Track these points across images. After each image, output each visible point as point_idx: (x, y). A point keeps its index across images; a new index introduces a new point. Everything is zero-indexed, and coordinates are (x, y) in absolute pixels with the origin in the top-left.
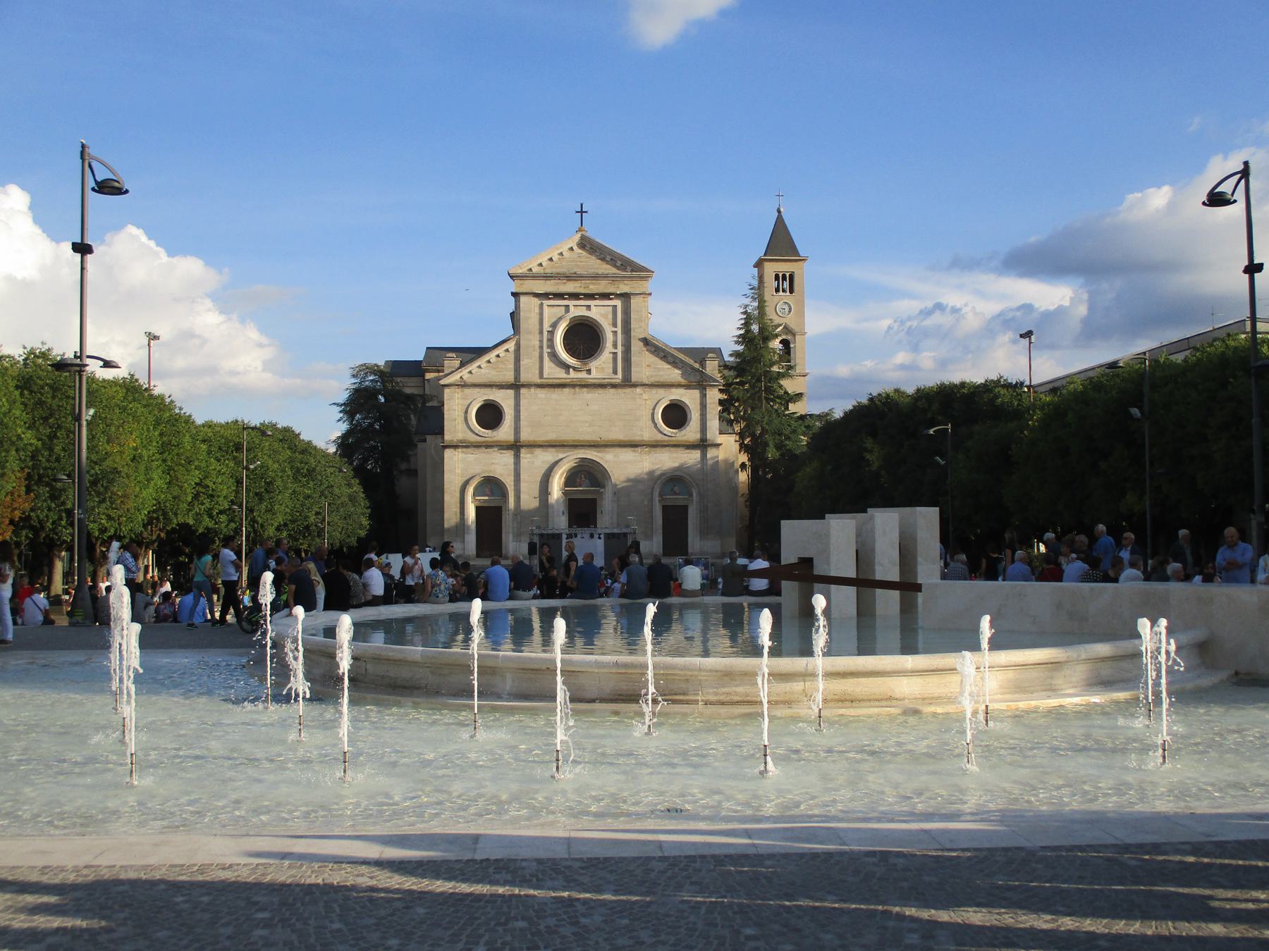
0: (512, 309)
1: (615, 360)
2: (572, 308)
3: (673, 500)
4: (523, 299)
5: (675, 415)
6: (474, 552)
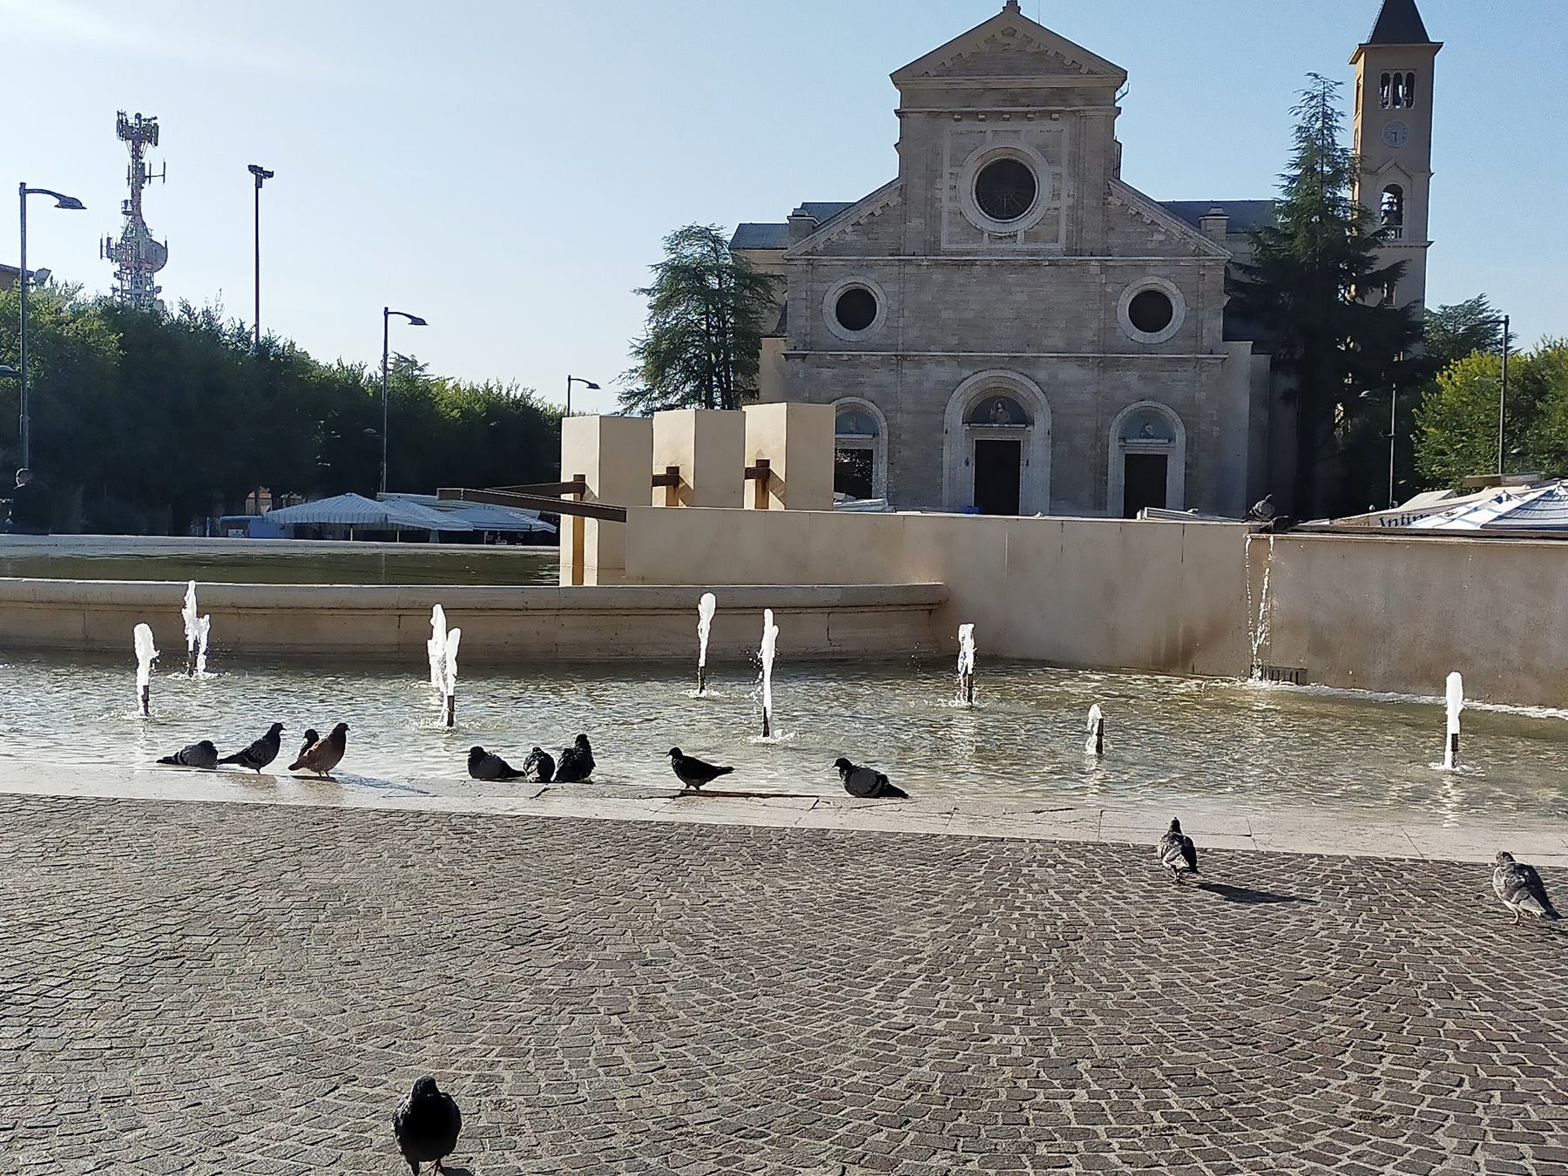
2: (989, 135)
3: (1141, 446)
5: (1150, 310)
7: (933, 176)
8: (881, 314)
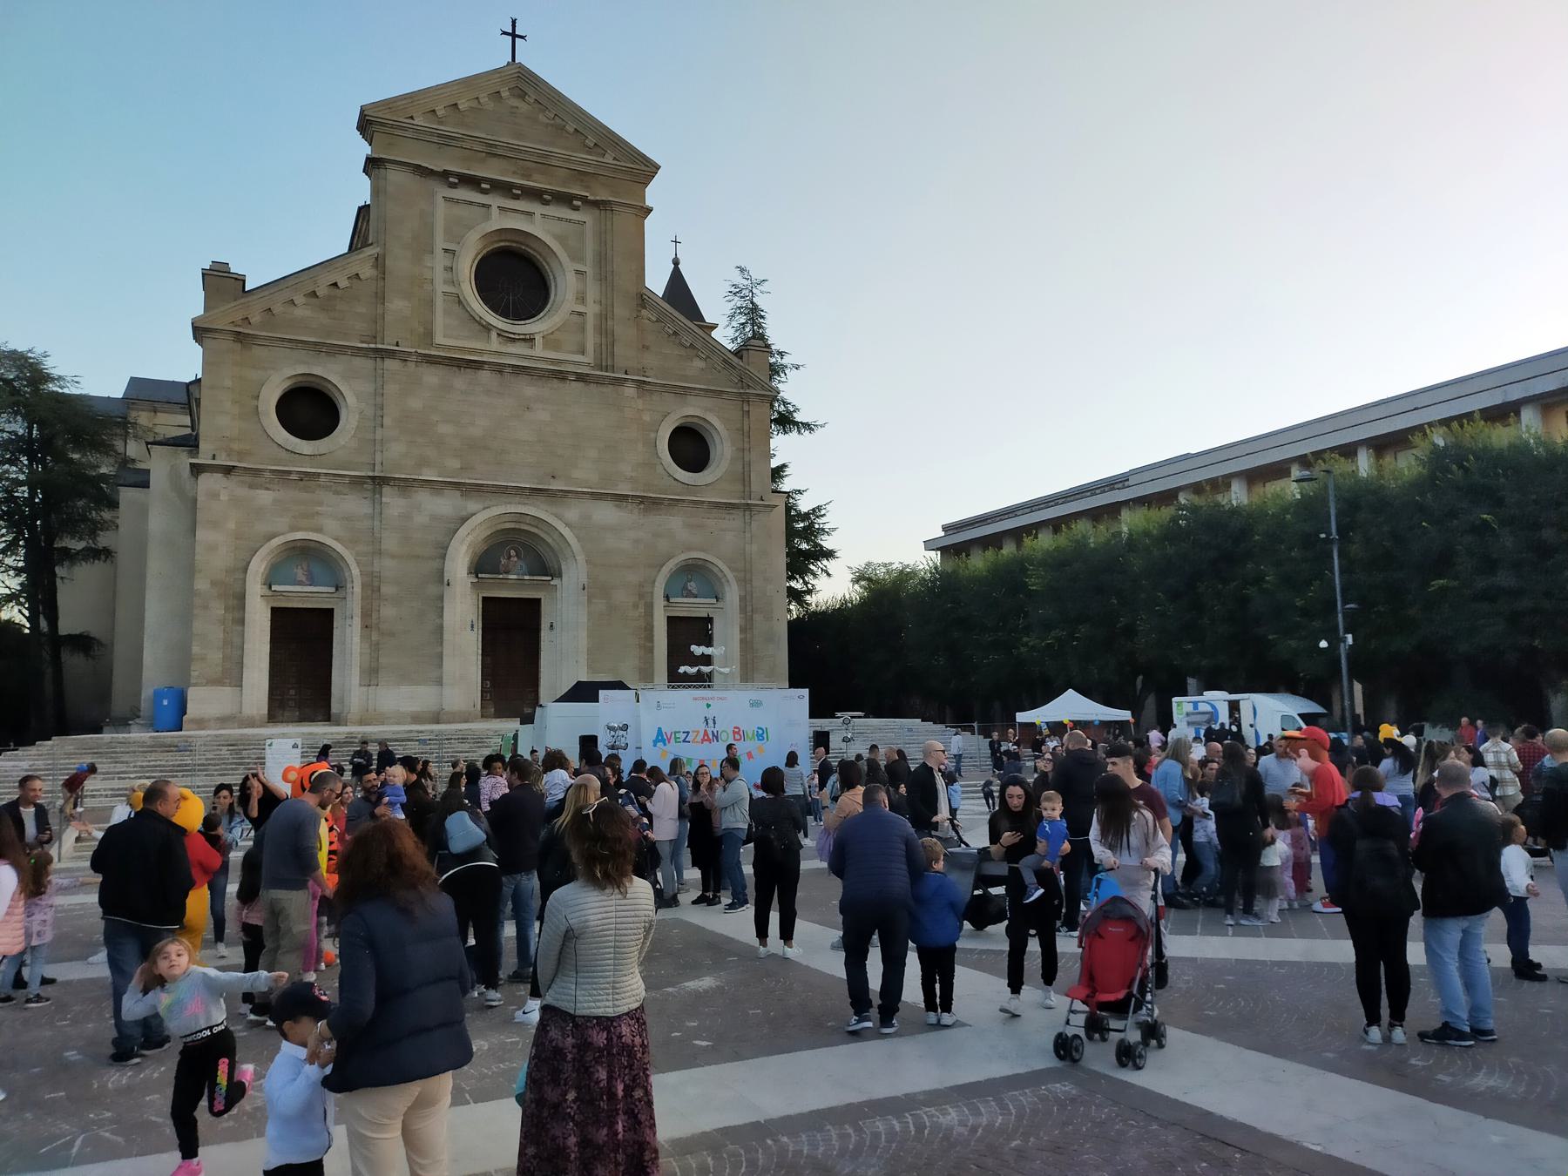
0: (365, 197)
1: (583, 330)
2: (495, 211)
4: (395, 176)
5: (690, 447)
6: (264, 710)
7: (423, 247)
8: (349, 420)
